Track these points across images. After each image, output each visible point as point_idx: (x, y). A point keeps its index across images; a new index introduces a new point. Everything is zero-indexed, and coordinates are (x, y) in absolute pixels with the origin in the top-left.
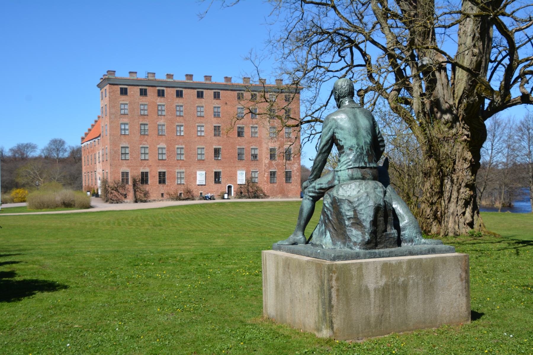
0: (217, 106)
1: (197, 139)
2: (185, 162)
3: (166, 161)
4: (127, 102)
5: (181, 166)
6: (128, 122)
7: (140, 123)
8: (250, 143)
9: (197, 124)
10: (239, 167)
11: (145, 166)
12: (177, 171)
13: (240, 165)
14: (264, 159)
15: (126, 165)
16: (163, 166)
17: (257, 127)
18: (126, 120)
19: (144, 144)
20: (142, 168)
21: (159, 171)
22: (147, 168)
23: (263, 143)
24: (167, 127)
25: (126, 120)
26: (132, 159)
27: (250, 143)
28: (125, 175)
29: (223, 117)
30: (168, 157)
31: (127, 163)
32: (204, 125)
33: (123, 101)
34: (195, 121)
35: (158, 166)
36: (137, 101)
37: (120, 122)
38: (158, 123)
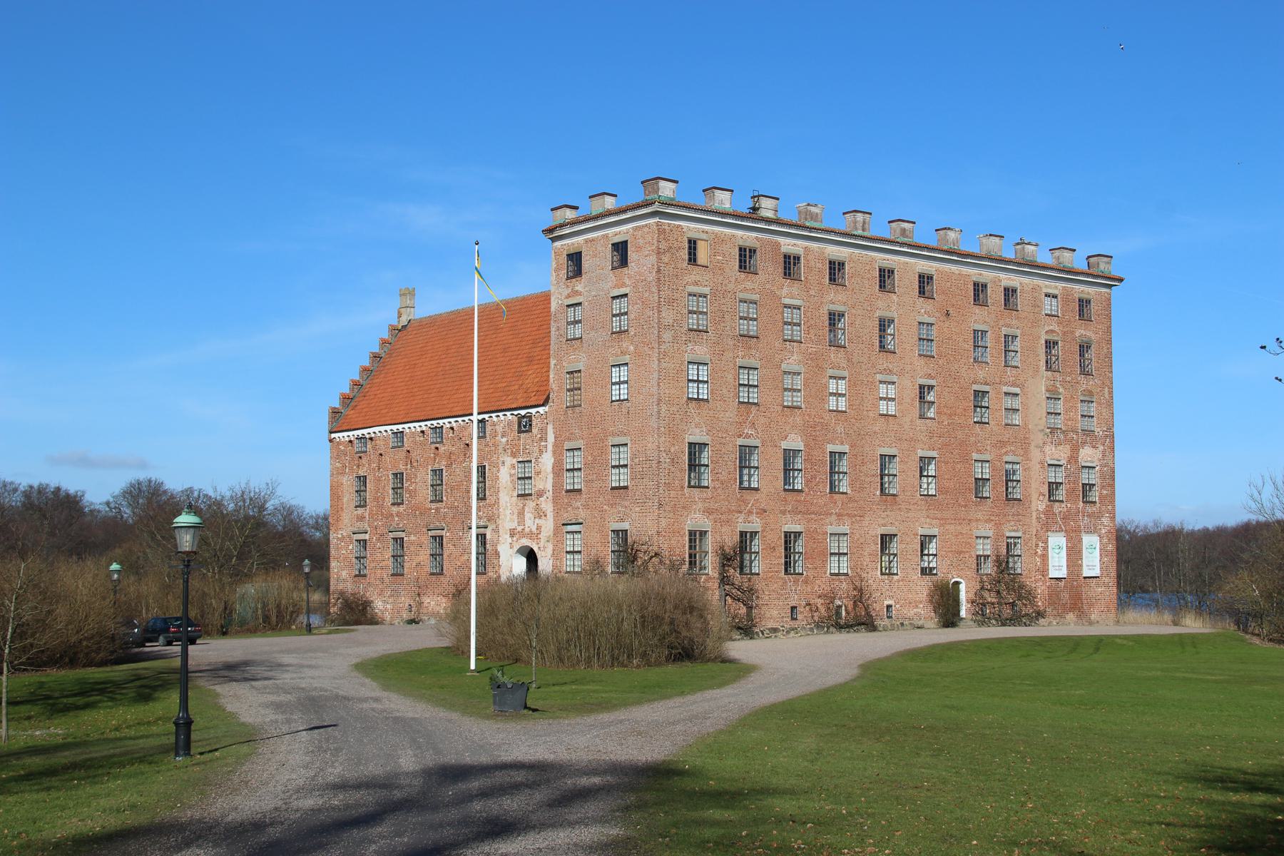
0: (927, 319)
1: (879, 425)
2: (851, 500)
3: (802, 497)
4: (706, 290)
5: (839, 515)
6: (707, 359)
7: (740, 362)
8: (1002, 443)
9: (879, 377)
10: (977, 520)
11: (750, 512)
12: (830, 529)
13: (980, 516)
14: (1034, 496)
15: (700, 505)
16: (795, 512)
17: (1017, 395)
18: (701, 351)
19: (748, 436)
20: (741, 518)
21: (786, 528)
22: (753, 517)
23: (1032, 447)
24: (806, 380)
25: (701, 351)
26: (717, 484)
27: (1002, 443)
28: (696, 537)
29: (940, 356)
30: (808, 482)
31: (704, 500)
32: (895, 379)
33: (696, 283)
34: (874, 366)
35: (783, 512)
36: (731, 287)
37: (687, 357)
38: (784, 366)
